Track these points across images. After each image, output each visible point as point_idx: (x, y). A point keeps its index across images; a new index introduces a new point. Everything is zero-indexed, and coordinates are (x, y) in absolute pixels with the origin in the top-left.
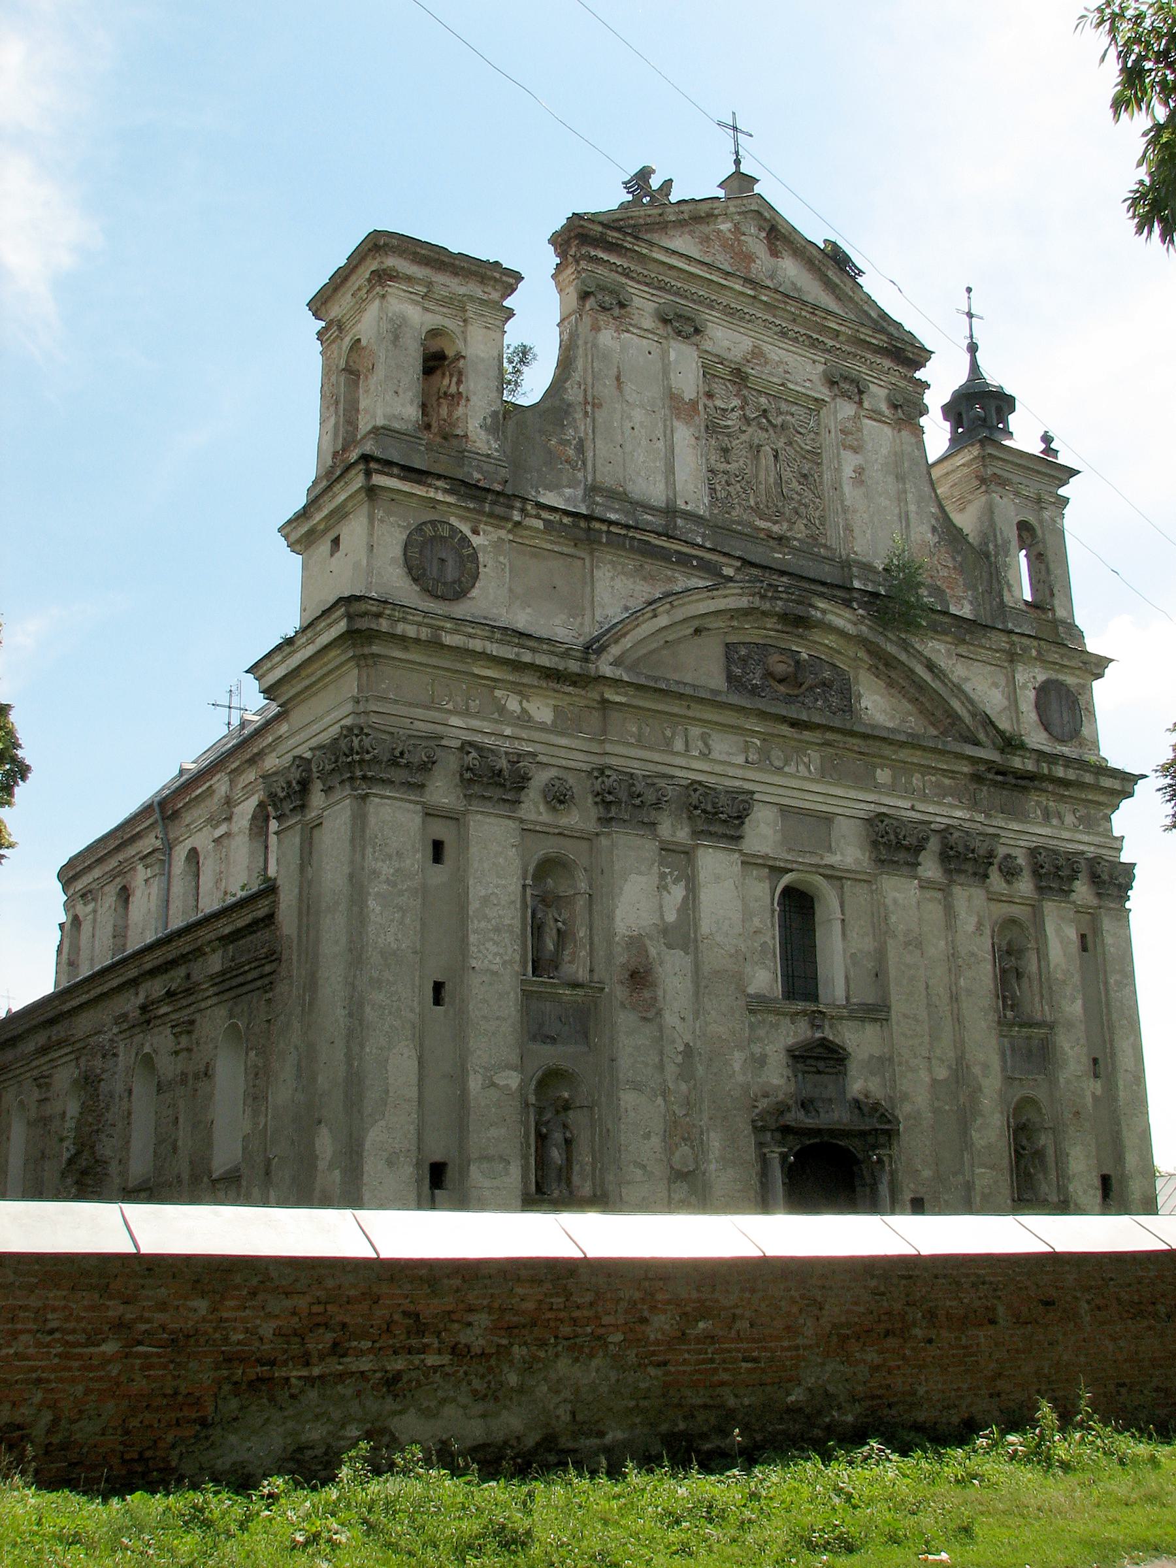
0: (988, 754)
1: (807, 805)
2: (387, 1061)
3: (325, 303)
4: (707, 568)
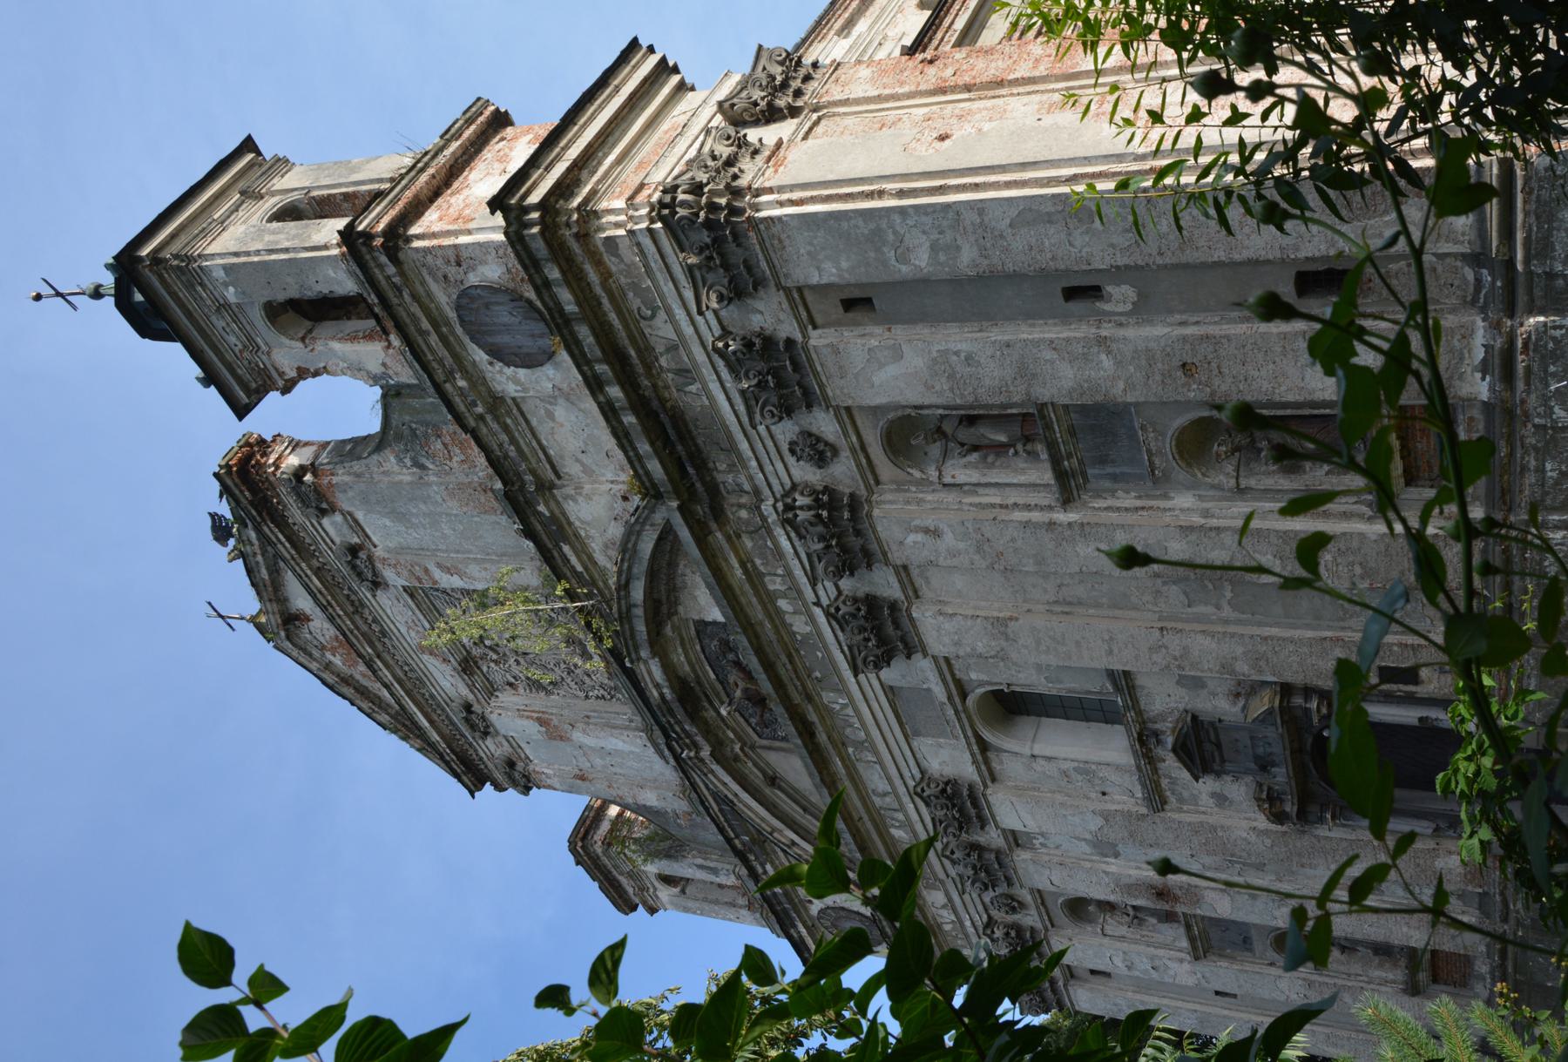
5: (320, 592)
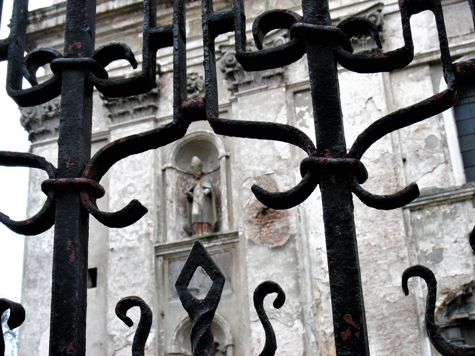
2: (38, 343)
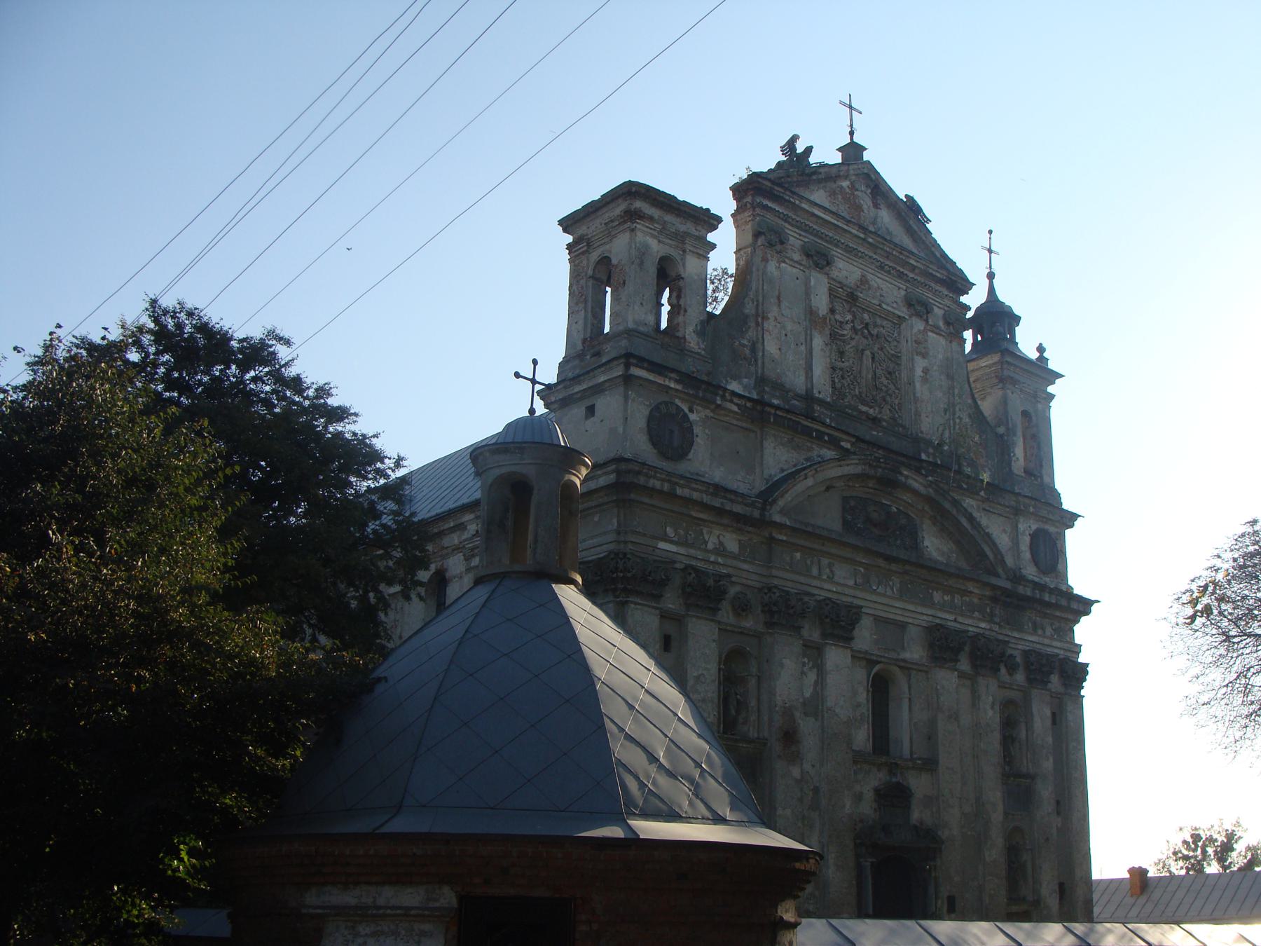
0: (1003, 583)
1: (891, 616)
3: (576, 222)
4: (834, 443)
5: (908, 257)
